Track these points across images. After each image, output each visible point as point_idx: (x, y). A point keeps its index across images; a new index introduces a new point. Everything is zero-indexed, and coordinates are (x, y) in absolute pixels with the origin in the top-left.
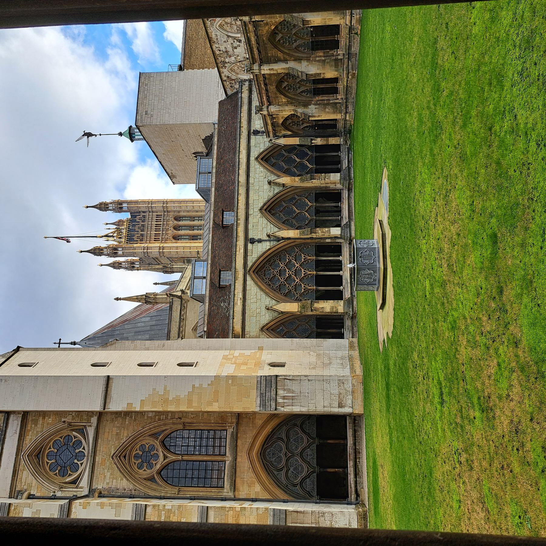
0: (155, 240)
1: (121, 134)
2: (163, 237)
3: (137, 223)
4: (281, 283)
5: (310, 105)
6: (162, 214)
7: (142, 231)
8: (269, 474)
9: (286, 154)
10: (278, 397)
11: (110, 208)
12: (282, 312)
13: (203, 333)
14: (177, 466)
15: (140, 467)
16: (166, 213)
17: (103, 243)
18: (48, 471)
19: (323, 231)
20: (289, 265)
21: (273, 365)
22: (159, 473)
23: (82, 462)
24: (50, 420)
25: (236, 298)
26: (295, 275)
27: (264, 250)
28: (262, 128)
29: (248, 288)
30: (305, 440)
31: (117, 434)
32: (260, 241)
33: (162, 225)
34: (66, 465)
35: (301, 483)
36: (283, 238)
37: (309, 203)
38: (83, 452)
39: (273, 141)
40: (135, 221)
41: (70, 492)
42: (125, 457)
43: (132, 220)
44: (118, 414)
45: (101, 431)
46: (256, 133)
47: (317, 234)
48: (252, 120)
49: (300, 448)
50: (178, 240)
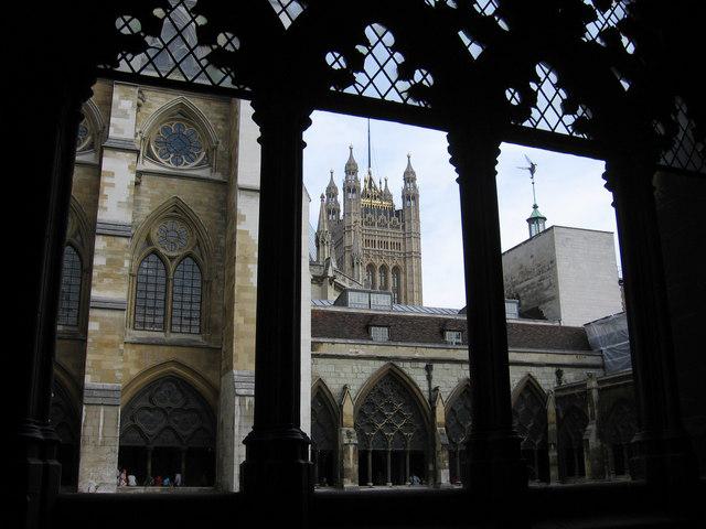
1: (535, 207)
12: (341, 406)
17: (362, 175)
22: (155, 252)
29: (372, 362)
31: (201, 202)
32: (429, 378)
36: (434, 408)
40: (392, 215)
43: (392, 212)
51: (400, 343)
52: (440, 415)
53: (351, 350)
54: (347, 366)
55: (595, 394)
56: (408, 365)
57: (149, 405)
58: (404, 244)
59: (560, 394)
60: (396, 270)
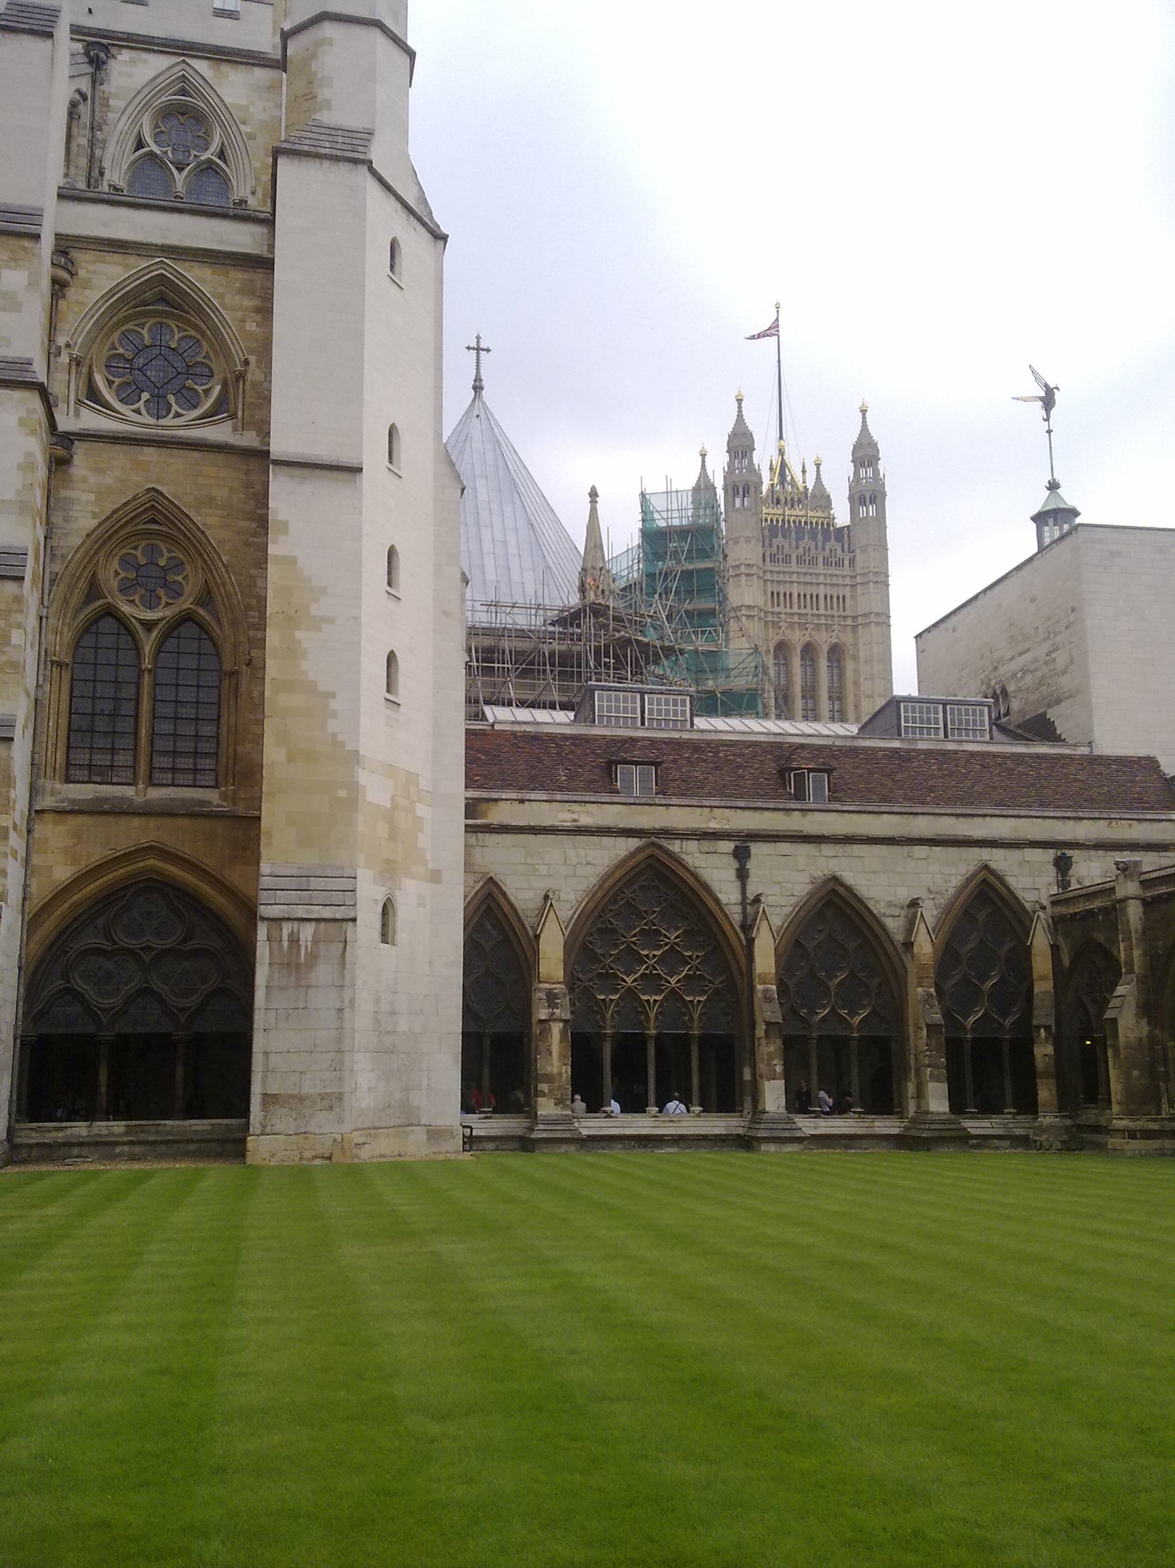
0: (772, 594)
1: (1053, 486)
2: (783, 616)
3: (820, 544)
4: (623, 936)
5: (1149, 1023)
6: (848, 613)
7: (800, 560)
8: (97, 903)
9: (1003, 951)
10: (296, 924)
11: (862, 472)
12: (537, 937)
13: (491, 720)
14: (127, 657)
15: (125, 562)
16: (849, 622)
17: (763, 457)
18: (123, 329)
19: (773, 1059)
20: (672, 958)
21: (387, 910)
22: (110, 612)
23: (143, 411)
24: (251, 326)
25: (575, 807)
26: (643, 974)
27: (715, 887)
28: (1079, 882)
29: (607, 841)
30: (183, 1003)
31: (211, 500)
32: (742, 875)
33: (815, 611)
34: (136, 372)
35: (69, 991)
36: (751, 941)
37: (857, 1020)
38: (168, 414)
39: (1041, 914)
40: (827, 538)
41: (63, 385)
42: (153, 521)
44: (262, 498)
45: (220, 458)
46: (1063, 865)
47: (763, 1041)
48: (1100, 853)
49: (164, 987)
50: (776, 657)
51: (674, 801)
52: (765, 961)
53: (561, 815)
54: (552, 850)
55: (1134, 911)
56: (692, 846)
57: (101, 942)
58: (853, 597)
59: (1062, 910)
60: (836, 653)
